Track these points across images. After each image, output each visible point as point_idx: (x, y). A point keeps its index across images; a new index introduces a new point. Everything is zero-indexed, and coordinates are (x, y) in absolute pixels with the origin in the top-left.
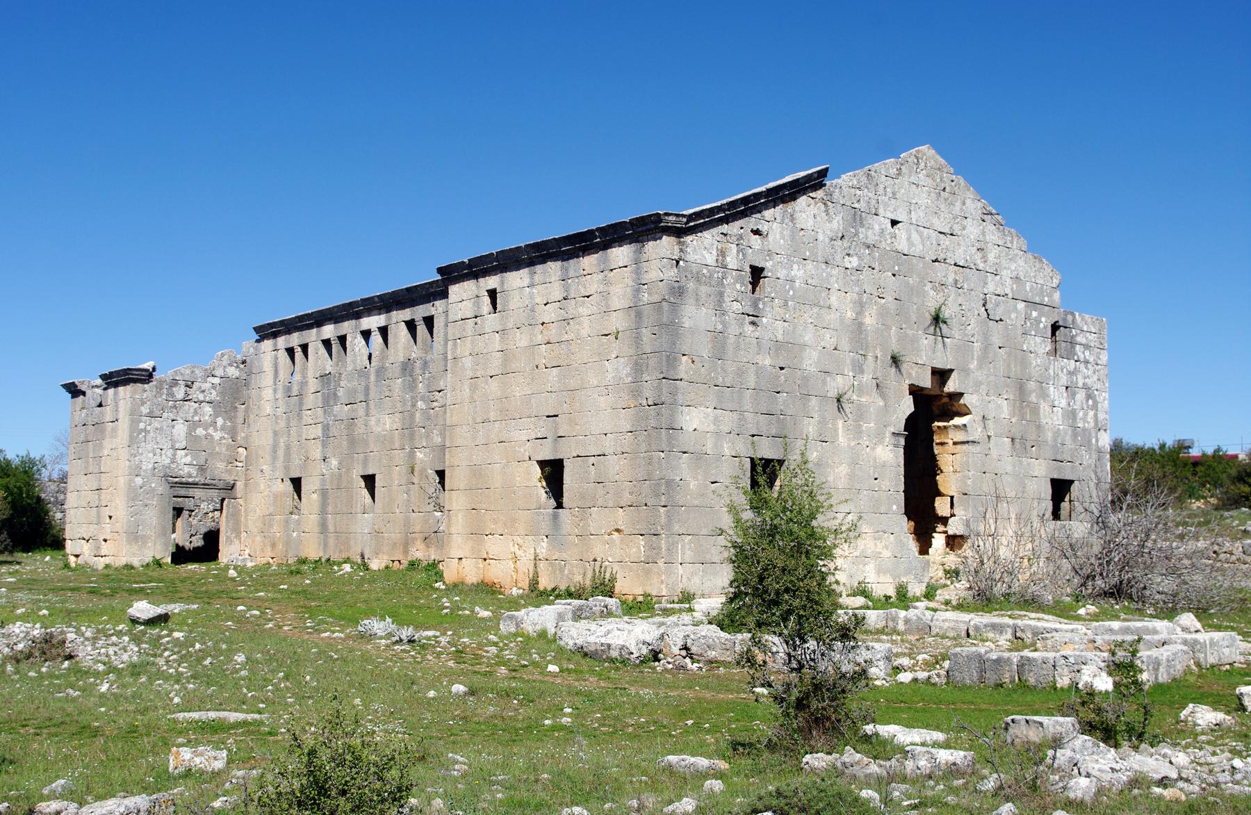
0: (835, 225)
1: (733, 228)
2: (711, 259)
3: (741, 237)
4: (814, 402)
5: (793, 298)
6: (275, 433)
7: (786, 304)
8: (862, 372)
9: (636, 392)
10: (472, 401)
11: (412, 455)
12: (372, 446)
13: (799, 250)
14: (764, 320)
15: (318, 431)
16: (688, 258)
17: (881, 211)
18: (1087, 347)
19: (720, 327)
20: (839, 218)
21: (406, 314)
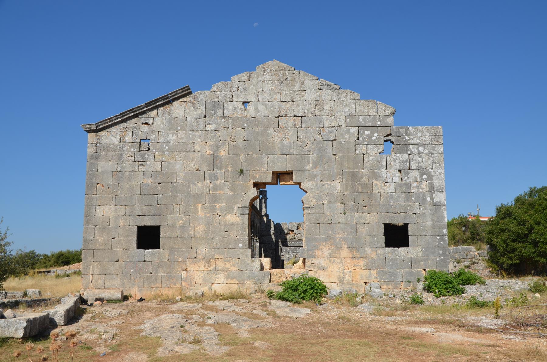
0: (199, 112)
1: (131, 123)
2: (116, 140)
3: (135, 127)
4: (180, 196)
5: (168, 150)
7: (163, 153)
8: (217, 179)
13: (173, 126)
14: (148, 163)
16: (102, 142)
17: (235, 99)
18: (423, 145)
19: (119, 169)
20: (203, 108)
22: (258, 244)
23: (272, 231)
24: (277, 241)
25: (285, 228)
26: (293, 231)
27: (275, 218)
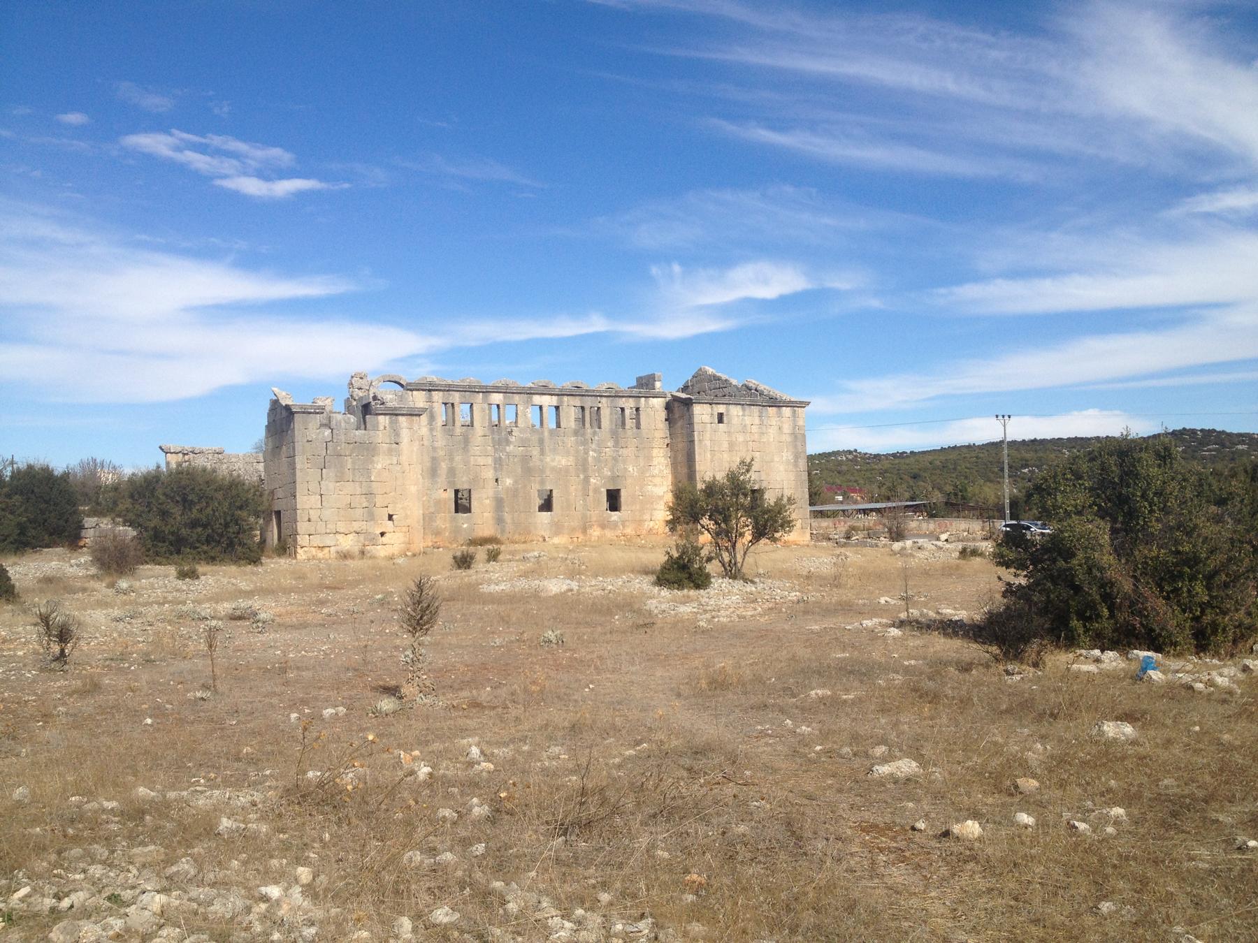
6: (434, 459)
9: (796, 464)
10: (712, 461)
11: (586, 480)
12: (548, 473)
15: (490, 461)
21: (577, 401)
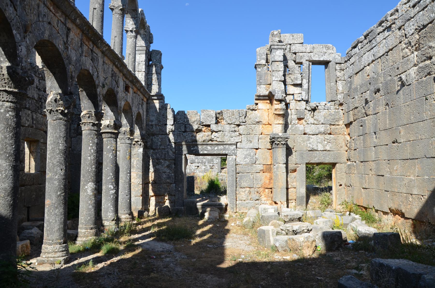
22: (139, 151)
23: (170, 126)
24: (178, 145)
25: (194, 121)
26: (209, 126)
27: (174, 104)
